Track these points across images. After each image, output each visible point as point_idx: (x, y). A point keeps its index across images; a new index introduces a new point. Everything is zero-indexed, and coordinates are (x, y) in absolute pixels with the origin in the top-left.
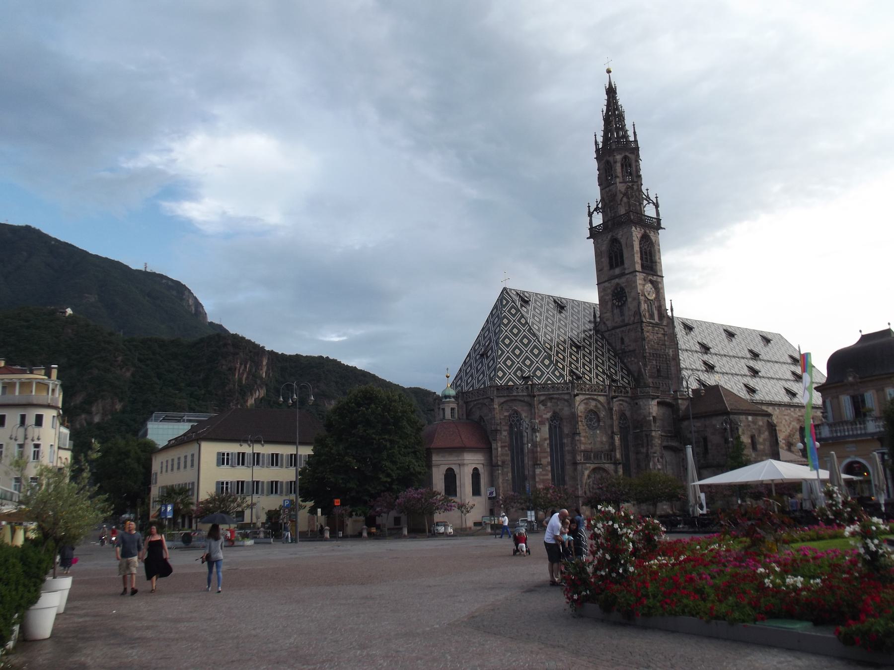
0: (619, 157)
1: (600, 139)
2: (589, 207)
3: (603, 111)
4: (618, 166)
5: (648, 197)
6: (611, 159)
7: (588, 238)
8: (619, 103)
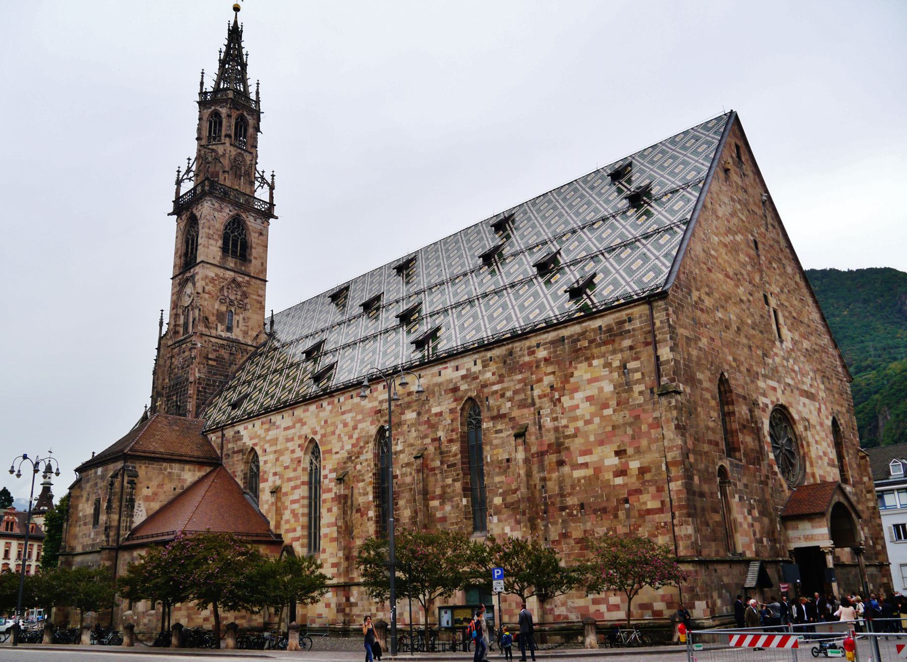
0: (235, 113)
1: (209, 86)
2: (179, 172)
3: (220, 52)
4: (233, 122)
5: (262, 177)
6: (224, 111)
7: (169, 214)
8: (244, 51)
